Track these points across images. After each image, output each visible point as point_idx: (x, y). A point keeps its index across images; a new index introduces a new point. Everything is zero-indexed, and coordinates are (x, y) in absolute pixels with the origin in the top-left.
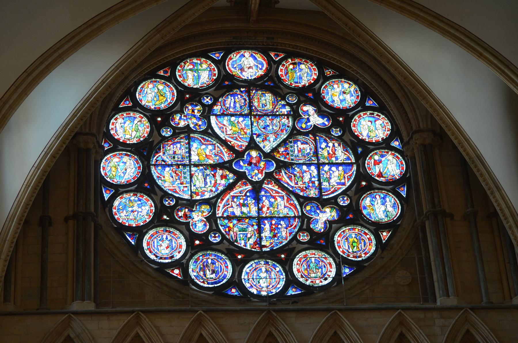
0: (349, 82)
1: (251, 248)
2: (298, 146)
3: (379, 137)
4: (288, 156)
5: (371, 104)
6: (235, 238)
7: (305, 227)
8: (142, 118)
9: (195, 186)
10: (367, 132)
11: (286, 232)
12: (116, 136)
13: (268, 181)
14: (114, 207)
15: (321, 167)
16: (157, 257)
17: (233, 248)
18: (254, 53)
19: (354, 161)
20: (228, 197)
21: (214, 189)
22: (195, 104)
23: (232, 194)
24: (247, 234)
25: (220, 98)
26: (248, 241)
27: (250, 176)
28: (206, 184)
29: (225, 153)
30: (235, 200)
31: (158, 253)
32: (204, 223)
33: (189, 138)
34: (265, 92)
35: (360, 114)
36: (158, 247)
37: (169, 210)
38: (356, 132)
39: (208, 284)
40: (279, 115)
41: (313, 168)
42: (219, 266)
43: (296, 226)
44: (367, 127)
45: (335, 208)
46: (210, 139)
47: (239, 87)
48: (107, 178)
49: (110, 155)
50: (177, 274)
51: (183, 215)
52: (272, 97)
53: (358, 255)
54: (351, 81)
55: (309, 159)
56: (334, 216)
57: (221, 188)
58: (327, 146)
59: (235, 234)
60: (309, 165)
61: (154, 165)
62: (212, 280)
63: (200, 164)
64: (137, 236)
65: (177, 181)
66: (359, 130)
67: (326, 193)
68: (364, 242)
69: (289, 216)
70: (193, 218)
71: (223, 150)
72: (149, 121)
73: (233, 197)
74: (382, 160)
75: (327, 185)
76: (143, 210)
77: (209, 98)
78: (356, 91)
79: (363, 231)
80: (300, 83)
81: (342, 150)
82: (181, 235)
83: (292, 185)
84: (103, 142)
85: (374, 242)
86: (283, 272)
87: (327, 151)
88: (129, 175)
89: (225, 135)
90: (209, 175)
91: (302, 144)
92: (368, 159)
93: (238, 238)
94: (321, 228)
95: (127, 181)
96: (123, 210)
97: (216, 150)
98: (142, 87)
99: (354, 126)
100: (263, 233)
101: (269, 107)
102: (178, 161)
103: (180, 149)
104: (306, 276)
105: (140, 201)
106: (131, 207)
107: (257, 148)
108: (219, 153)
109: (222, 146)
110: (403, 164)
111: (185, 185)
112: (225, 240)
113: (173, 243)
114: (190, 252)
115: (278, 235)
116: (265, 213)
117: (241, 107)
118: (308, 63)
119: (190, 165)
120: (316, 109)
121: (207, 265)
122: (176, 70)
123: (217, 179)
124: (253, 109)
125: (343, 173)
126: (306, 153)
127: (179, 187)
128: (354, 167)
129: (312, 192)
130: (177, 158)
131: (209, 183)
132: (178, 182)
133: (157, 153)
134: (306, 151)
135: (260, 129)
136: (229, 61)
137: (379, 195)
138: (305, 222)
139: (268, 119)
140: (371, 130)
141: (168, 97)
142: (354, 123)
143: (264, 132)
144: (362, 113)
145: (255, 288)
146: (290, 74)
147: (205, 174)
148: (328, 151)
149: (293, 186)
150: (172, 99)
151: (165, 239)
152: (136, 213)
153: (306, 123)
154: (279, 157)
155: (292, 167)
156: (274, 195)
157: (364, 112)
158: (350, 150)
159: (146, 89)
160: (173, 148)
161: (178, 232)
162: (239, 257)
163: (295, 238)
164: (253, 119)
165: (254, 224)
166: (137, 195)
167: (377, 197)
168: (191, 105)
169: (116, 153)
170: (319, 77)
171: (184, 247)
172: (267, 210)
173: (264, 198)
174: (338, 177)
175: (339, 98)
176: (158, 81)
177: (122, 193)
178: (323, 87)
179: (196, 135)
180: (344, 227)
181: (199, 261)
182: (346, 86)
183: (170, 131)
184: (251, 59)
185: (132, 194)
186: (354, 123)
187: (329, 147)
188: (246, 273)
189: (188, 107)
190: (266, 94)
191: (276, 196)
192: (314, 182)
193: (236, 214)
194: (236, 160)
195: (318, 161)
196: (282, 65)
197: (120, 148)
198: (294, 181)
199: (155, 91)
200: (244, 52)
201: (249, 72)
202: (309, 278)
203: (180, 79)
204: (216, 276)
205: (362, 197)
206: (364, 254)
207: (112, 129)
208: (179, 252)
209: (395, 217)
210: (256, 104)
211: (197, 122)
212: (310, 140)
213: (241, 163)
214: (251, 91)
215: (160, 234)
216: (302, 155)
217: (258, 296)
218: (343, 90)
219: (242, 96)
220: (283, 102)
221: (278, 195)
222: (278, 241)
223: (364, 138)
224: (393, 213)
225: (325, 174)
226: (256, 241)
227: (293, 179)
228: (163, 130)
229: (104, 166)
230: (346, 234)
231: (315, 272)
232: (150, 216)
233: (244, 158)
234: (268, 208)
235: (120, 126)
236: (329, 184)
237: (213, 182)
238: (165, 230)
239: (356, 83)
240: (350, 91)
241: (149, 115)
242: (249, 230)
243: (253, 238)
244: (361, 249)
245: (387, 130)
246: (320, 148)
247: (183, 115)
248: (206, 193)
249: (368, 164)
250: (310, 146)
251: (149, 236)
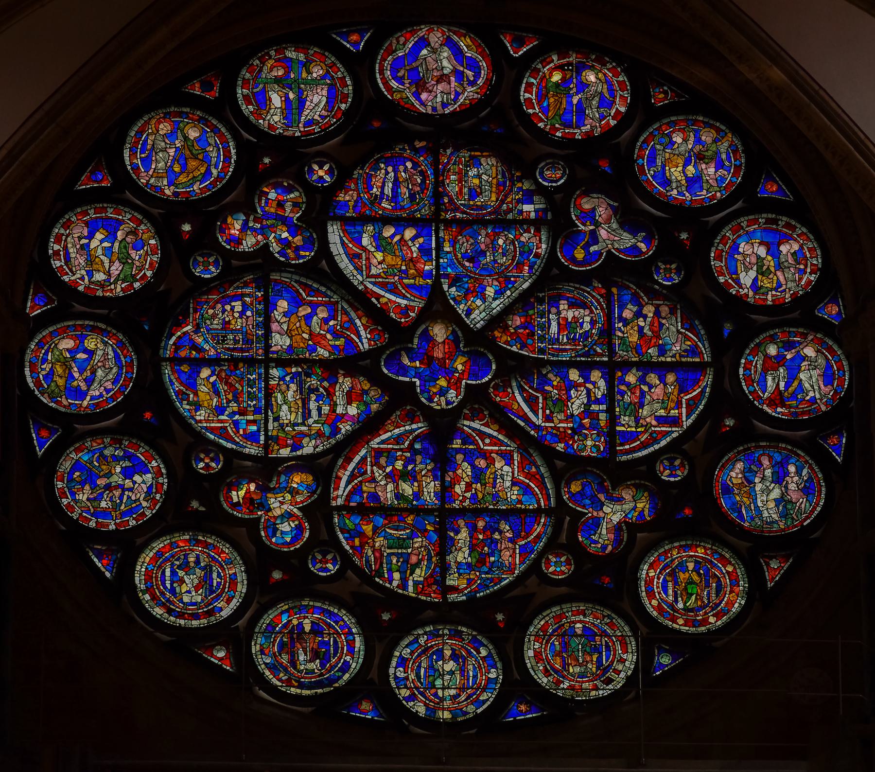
0: (718, 124)
1: (417, 594)
2: (558, 313)
3: (784, 291)
4: (530, 341)
5: (772, 193)
6: (378, 566)
7: (563, 538)
8: (139, 222)
9: (277, 419)
10: (753, 274)
11: (511, 551)
12: (67, 274)
13: (472, 410)
14: (59, 474)
15: (620, 374)
16: (170, 612)
17: (372, 591)
18: (455, 33)
19: (710, 360)
20: (363, 452)
21: (327, 430)
22: (286, 184)
23: (375, 443)
24: (409, 555)
25: (355, 169)
26: (411, 574)
27: (426, 395)
28: (307, 414)
29: (361, 329)
30: (383, 461)
31: (173, 603)
32: (297, 523)
33: (263, 283)
34: (479, 154)
35: (739, 221)
36: (175, 585)
37: (206, 484)
38: (723, 275)
39: (301, 686)
40: (515, 222)
41: (596, 375)
42: (332, 639)
43: (538, 537)
44: (754, 260)
45: (645, 488)
46: (323, 289)
47: (409, 138)
48: (42, 394)
49: (51, 329)
50: (220, 659)
51: (243, 499)
52: (497, 167)
53: (698, 618)
54: (721, 123)
55: (587, 349)
56: (643, 511)
57: (345, 428)
58: (639, 314)
59: (377, 555)
60: (585, 369)
61: (171, 360)
62: (311, 678)
63: (294, 359)
64: (119, 555)
65: (230, 405)
66: (733, 269)
67: (627, 447)
68: (719, 583)
69: (523, 507)
70: (270, 510)
71: (357, 321)
72: (157, 233)
73: (378, 453)
74: (788, 357)
75: (630, 423)
76: (137, 485)
77: (326, 167)
78: (735, 152)
79: (716, 552)
80: (578, 127)
81: (680, 328)
82: (236, 554)
83: (538, 421)
84: (32, 291)
85: (743, 585)
86: (497, 659)
87: (636, 328)
88: (103, 388)
89: (365, 277)
90: (317, 390)
91: (571, 306)
92: (749, 355)
93: (385, 566)
94: (606, 542)
95: (97, 405)
96: (83, 483)
97: (339, 319)
98: (140, 132)
99: (719, 258)
100: (451, 552)
101: (488, 198)
102: (234, 350)
103: (242, 313)
104: (556, 671)
105: (129, 461)
106: (104, 476)
107: (450, 316)
108: (347, 329)
109: (356, 310)
110: (844, 372)
111: (251, 418)
112: (349, 571)
113: (215, 575)
114: (258, 602)
115: (492, 559)
116: (461, 498)
117: (412, 197)
118: (604, 64)
119: (267, 362)
120: (616, 204)
121: (299, 635)
122: (237, 80)
123: (338, 403)
124: (444, 204)
125: (676, 393)
126: (581, 332)
127: (236, 424)
128: (707, 376)
129: (589, 443)
130: (232, 342)
131: (314, 413)
132: (234, 406)
133: (180, 326)
134: (582, 327)
135: (459, 262)
136: (384, 59)
137: (768, 455)
138: (566, 526)
139: (483, 232)
140: (765, 268)
141: (214, 160)
142: (721, 247)
143: (471, 272)
144: (746, 218)
145: (421, 701)
146: (552, 100)
147: (306, 387)
148: (641, 329)
149: (539, 426)
150: (225, 170)
151: (192, 565)
152: (117, 493)
153: (586, 247)
154: (507, 343)
155: (540, 374)
156: (486, 448)
157: (751, 217)
158: (700, 327)
159: (152, 138)
160: (224, 311)
161: (228, 546)
162: (386, 617)
163: (535, 569)
164: (441, 234)
165: (429, 527)
166: (121, 444)
167: (766, 462)
168: (275, 186)
169: (66, 324)
170: (631, 107)
171: (242, 588)
172: (466, 492)
173: (460, 457)
174: (663, 403)
175: (684, 172)
176: (187, 113)
177: (83, 437)
178: (642, 139)
179: (285, 278)
180: (667, 542)
181: (280, 625)
182: (707, 137)
183: (216, 264)
184: (446, 53)
185: (109, 440)
187: (645, 317)
188: (399, 662)
189: (268, 193)
190: (483, 160)
191: (492, 451)
192: (598, 414)
193: (382, 499)
194: (391, 350)
195: (609, 356)
196: (532, 71)
197: (78, 308)
198: (544, 412)
199: (177, 142)
200: (431, 30)
201: (438, 91)
202: (564, 677)
203: (247, 109)
204: (323, 665)
205: (724, 461)
206: (712, 615)
207: (57, 253)
208: (229, 601)
209: (805, 520)
210: (453, 188)
211: (290, 238)
212: (593, 297)
213: (406, 361)
214: (441, 151)
215: (182, 551)
216: (568, 339)
217: (430, 723)
218: (698, 148)
219: (416, 165)
220: (526, 186)
221: (497, 448)
222: (490, 576)
223: (742, 292)
224: (803, 505)
225: (629, 394)
226: (431, 575)
227: (541, 405)
228: (195, 260)
229: (34, 360)
230: (673, 560)
231: (581, 660)
232: (154, 502)
233: (413, 344)
234: (468, 487)
235: (78, 247)
236: (637, 420)
237: (326, 409)
238: (195, 540)
239: (736, 128)
240: (718, 153)
241: (159, 213)
242: (416, 545)
243: (425, 567)
244: (709, 602)
245: (809, 270)
246: (621, 319)
247: (252, 217)
248: (305, 441)
249: (745, 369)
250: (592, 312)
251: (151, 554)
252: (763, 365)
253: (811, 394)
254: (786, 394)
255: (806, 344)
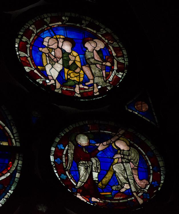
3: (92, 85)
10: (59, 67)
44: (59, 54)
66: (38, 60)
74: (100, 148)
92: (59, 143)
99: (23, 48)
140: (71, 62)
142: (24, 39)
186: (24, 39)
245: (115, 68)
252: (74, 154)
253: (127, 186)
254: (100, 184)
255: (117, 137)
